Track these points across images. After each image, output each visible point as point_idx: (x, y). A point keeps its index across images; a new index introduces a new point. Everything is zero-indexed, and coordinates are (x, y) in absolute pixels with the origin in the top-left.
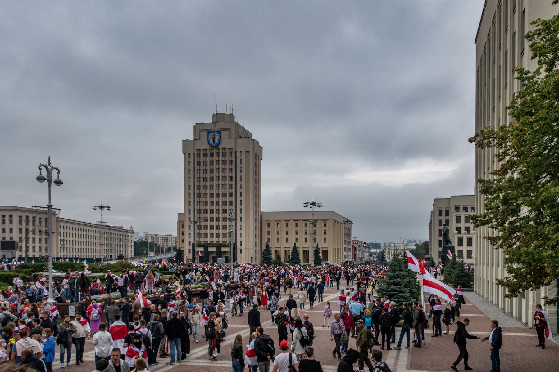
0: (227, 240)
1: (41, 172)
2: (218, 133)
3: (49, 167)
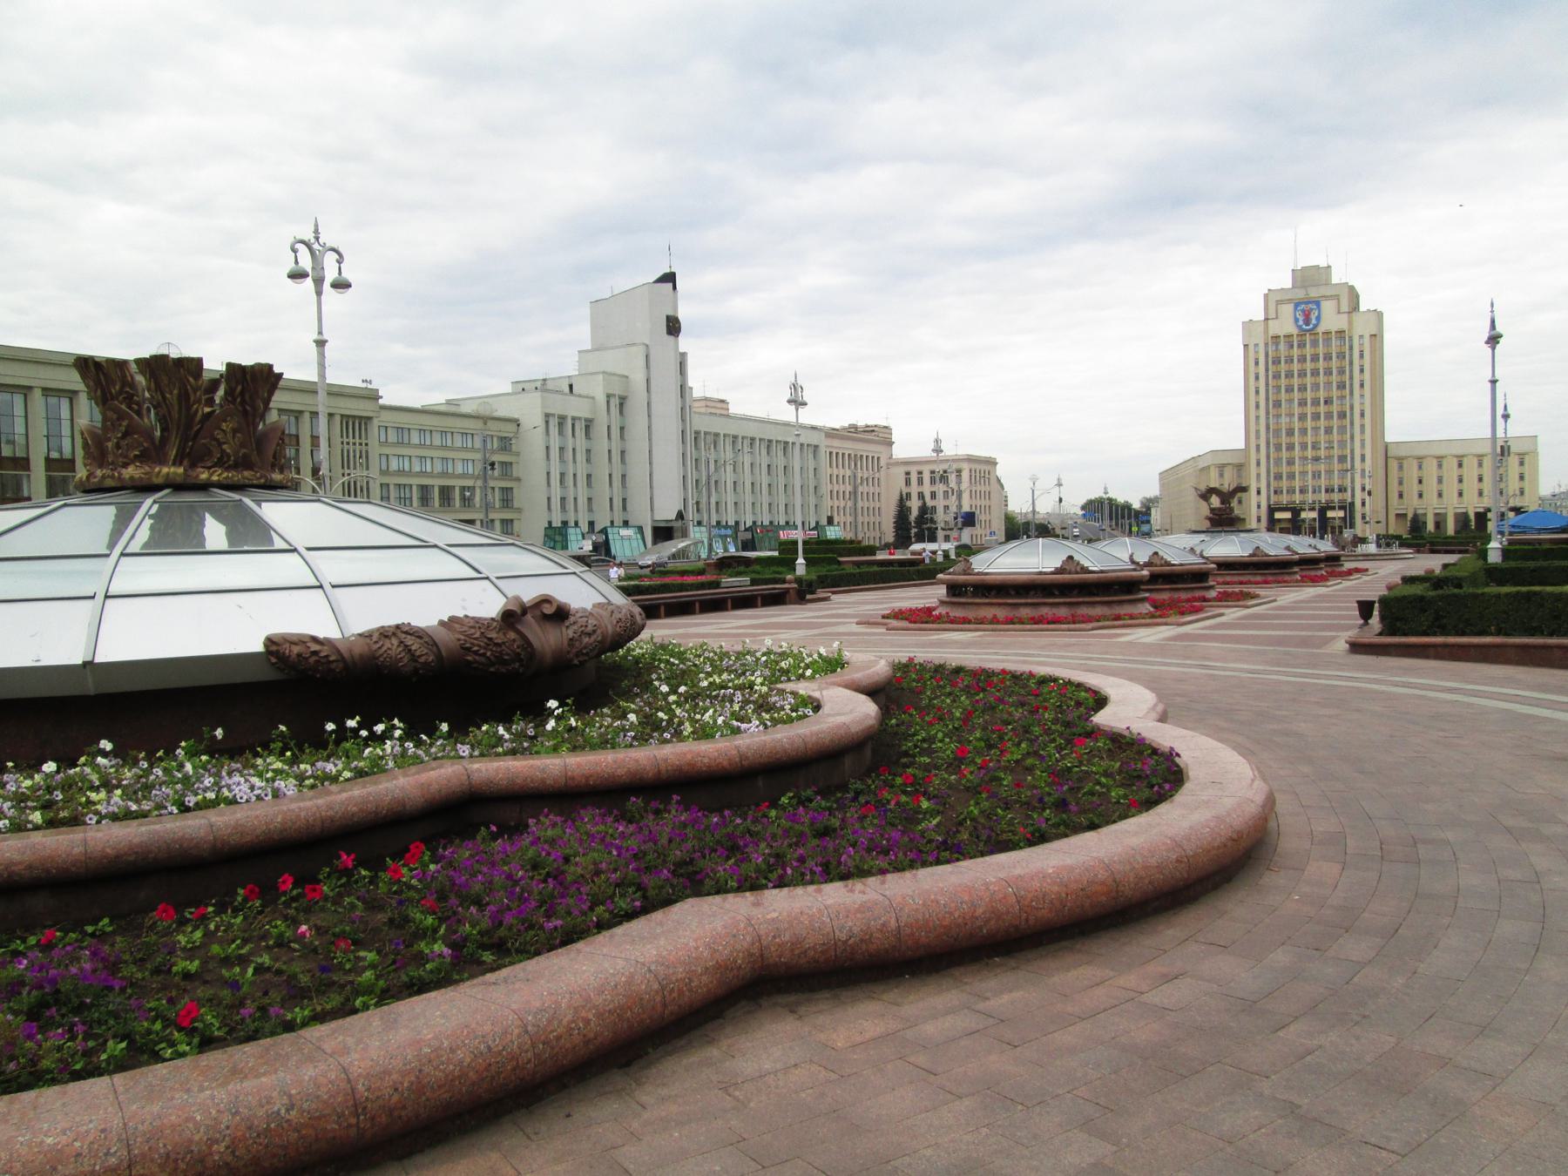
0: (1336, 497)
1: (296, 257)
3: (316, 246)
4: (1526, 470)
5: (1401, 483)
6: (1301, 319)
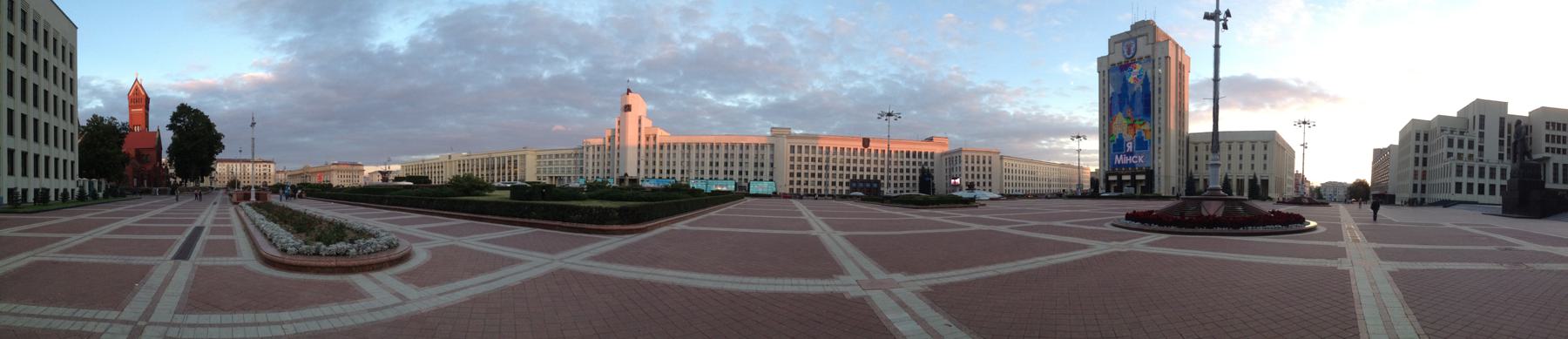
4: (1267, 152)
5: (1196, 159)
6: (1126, 50)
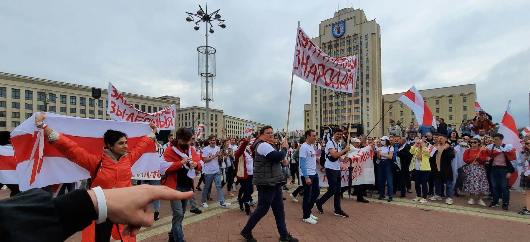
2: (343, 24)
